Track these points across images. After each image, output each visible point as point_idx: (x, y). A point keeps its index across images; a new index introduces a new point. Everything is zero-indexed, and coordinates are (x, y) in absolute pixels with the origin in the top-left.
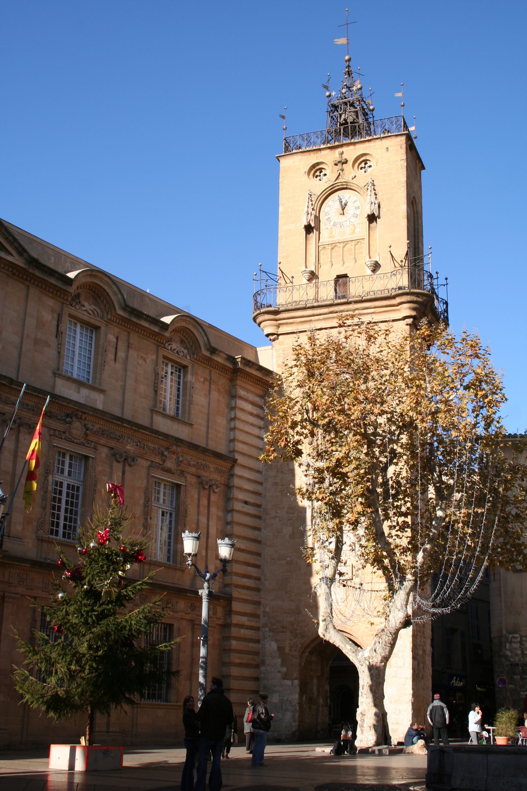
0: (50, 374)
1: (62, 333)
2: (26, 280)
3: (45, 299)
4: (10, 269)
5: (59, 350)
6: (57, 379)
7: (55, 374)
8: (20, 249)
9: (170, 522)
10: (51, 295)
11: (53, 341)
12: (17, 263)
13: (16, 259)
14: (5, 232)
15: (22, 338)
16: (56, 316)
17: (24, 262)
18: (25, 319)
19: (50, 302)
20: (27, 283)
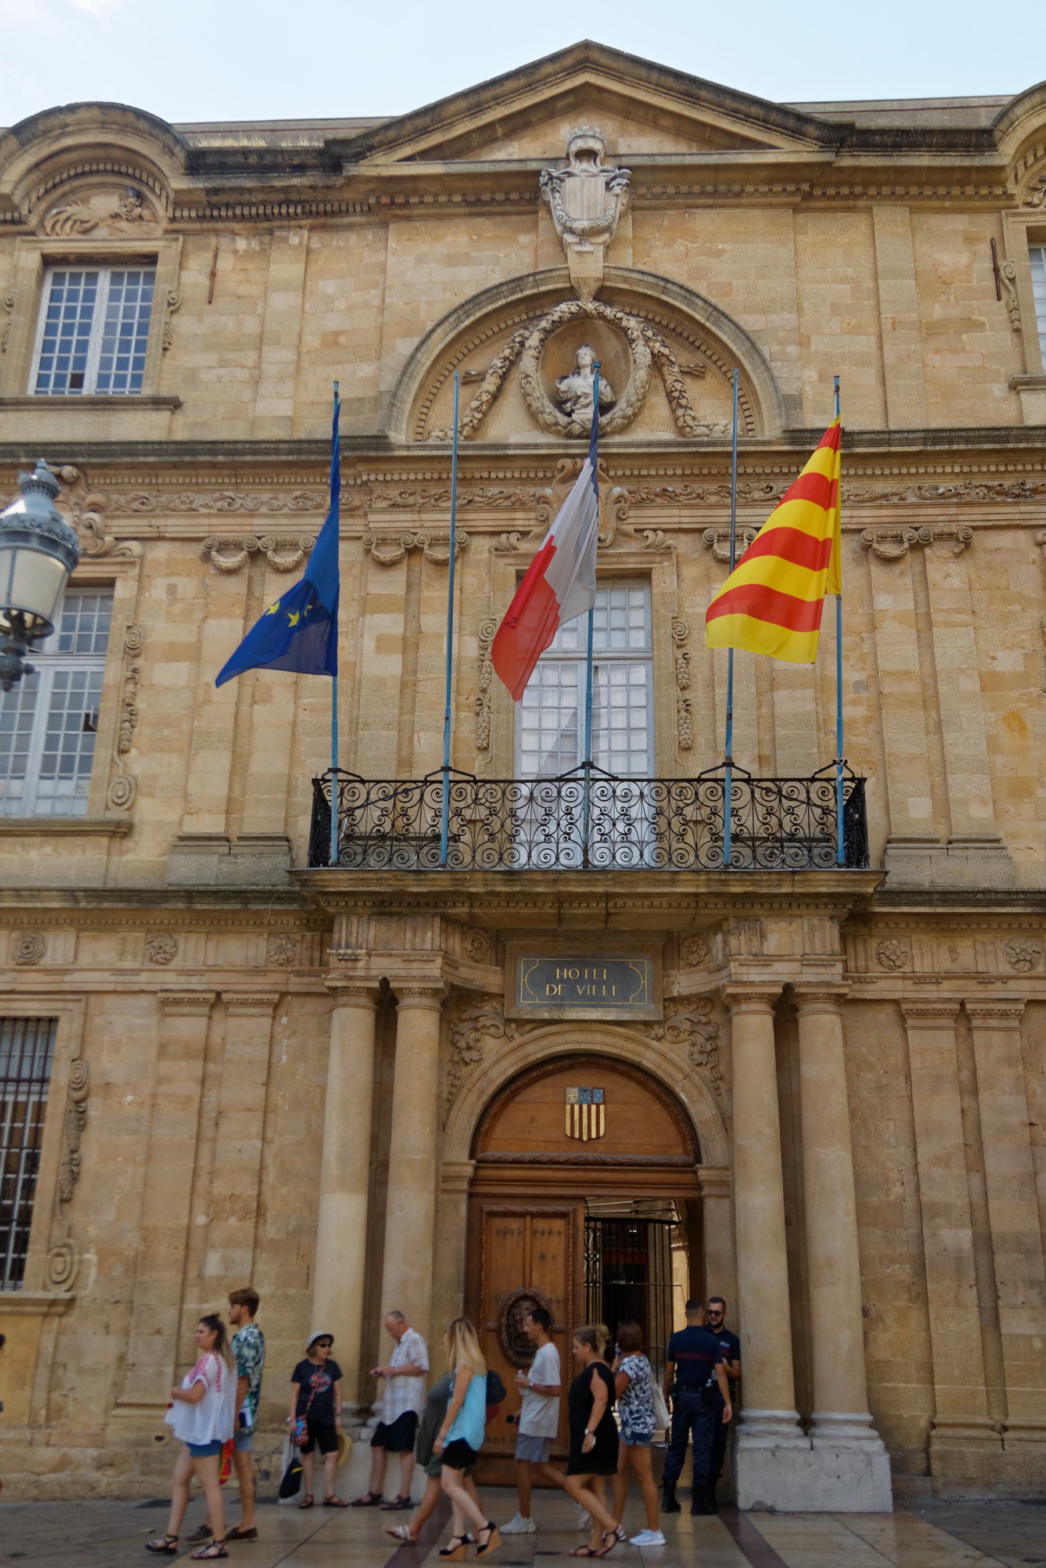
0: (999, 389)
1: (1012, 280)
2: (852, 195)
3: (934, 221)
4: (791, 188)
5: (1016, 324)
6: (1024, 396)
7: (1014, 386)
8: (791, 123)
9: (536, 446)
10: (947, 204)
11: (992, 312)
12: (792, 159)
13: (788, 152)
14: (735, 105)
15: (880, 336)
16: (985, 248)
17: (817, 148)
18: (877, 288)
19: (959, 223)
20: (861, 203)
